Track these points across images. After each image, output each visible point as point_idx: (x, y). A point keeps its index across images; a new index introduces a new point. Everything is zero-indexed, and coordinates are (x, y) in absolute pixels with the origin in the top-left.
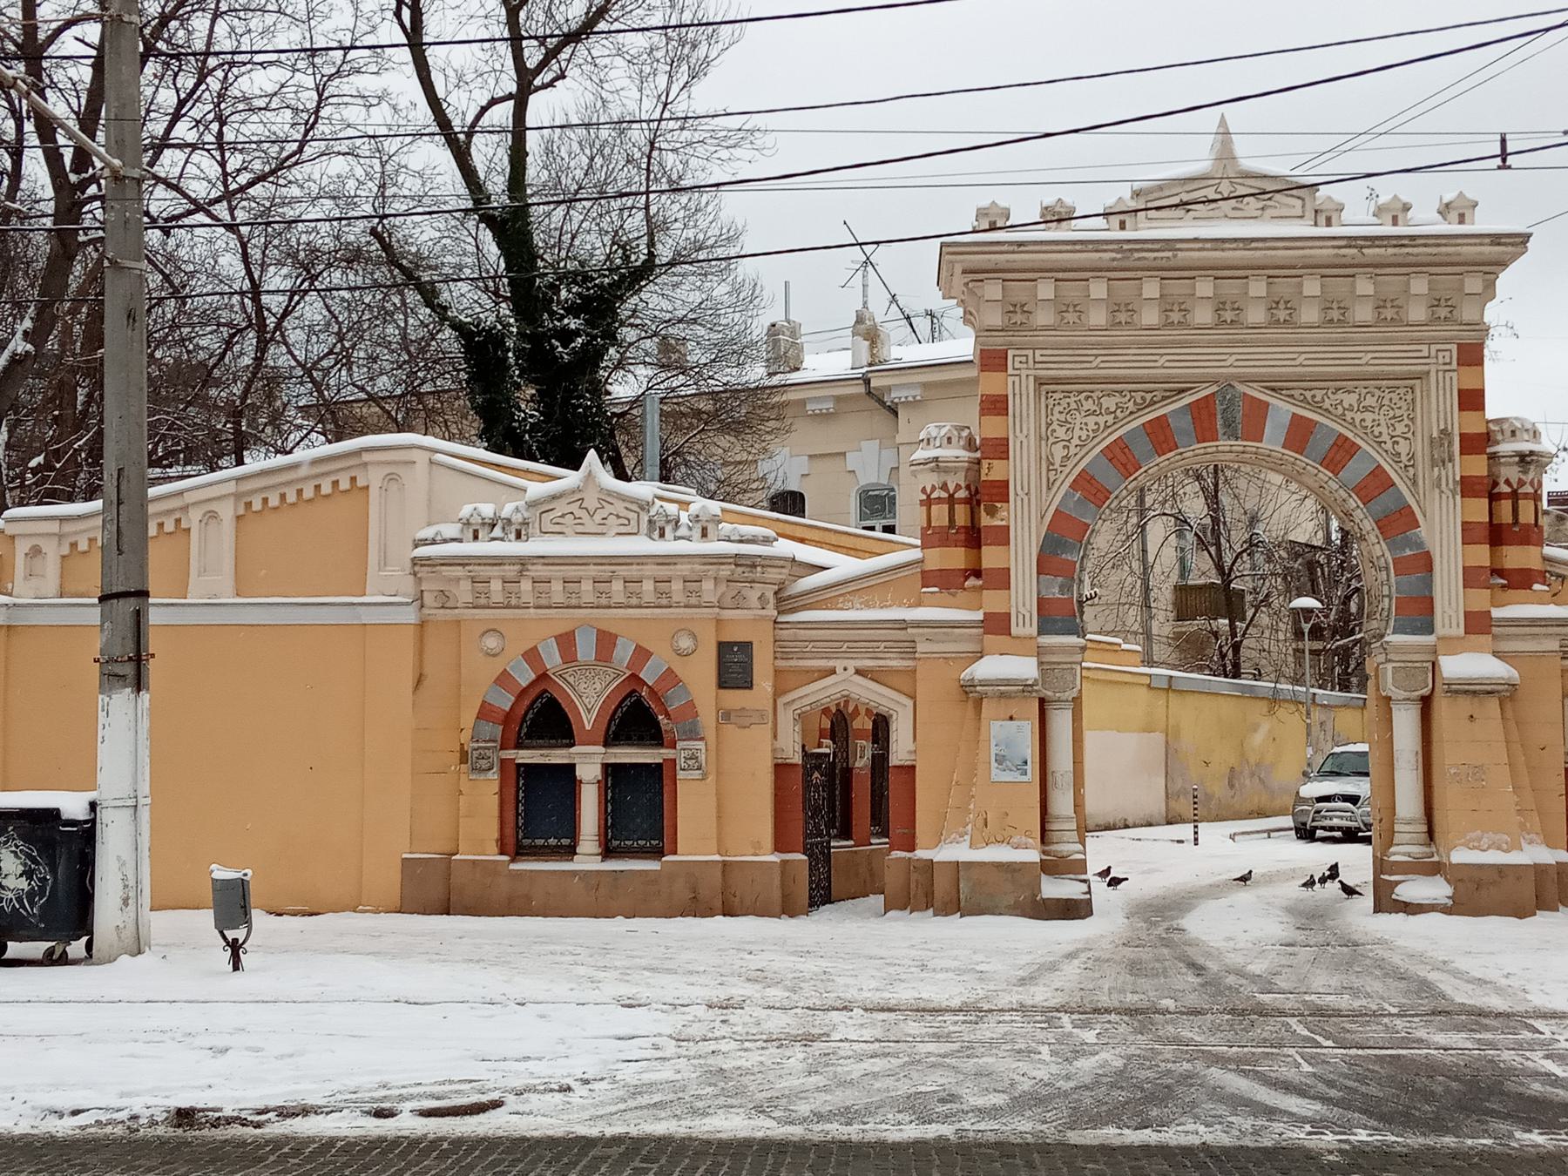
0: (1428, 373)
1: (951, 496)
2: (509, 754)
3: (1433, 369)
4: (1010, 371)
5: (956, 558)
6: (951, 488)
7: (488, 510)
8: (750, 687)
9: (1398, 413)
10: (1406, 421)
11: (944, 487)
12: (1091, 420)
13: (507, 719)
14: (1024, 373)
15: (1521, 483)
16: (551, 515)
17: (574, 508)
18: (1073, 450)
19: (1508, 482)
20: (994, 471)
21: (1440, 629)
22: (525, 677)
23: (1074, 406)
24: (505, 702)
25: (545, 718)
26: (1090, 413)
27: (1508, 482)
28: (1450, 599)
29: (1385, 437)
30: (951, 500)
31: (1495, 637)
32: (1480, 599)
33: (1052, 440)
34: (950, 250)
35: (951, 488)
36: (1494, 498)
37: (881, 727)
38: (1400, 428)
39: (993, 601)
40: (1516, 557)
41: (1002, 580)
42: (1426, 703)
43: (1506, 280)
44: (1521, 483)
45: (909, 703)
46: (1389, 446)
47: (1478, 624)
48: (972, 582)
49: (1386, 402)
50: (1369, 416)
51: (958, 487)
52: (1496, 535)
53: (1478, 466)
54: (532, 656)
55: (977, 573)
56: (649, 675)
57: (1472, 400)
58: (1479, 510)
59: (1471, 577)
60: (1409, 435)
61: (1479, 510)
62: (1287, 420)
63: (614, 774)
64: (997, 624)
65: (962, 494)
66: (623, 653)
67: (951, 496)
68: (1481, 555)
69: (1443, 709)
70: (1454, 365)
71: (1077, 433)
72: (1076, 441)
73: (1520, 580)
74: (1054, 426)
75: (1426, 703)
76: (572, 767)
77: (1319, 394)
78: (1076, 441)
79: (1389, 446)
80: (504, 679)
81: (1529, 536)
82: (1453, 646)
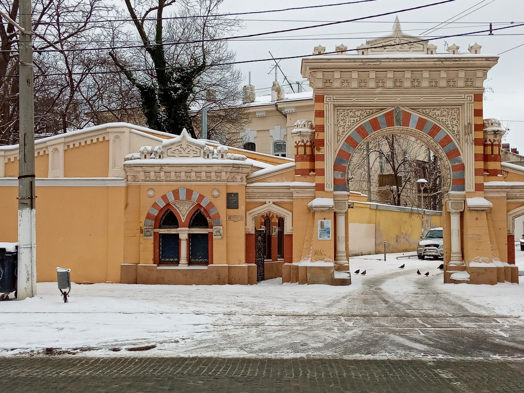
0: (464, 103)
1: (305, 144)
2: (157, 230)
3: (466, 102)
4: (325, 102)
5: (306, 165)
6: (305, 142)
7: (149, 148)
8: (238, 208)
10: (457, 120)
11: (303, 141)
12: (352, 119)
13: (156, 219)
14: (329, 103)
15: (494, 141)
16: (171, 150)
17: (179, 148)
18: (346, 129)
19: (490, 140)
20: (319, 136)
21: (467, 189)
22: (162, 204)
23: (346, 114)
24: (155, 213)
25: (169, 218)
26: (352, 117)
27: (490, 140)
28: (470, 179)
29: (450, 125)
30: (305, 146)
31: (485, 192)
32: (480, 179)
33: (339, 126)
34: (305, 61)
35: (305, 142)
36: (485, 146)
37: (281, 222)
38: (455, 122)
39: (319, 180)
40: (492, 165)
41: (322, 172)
42: (462, 214)
43: (490, 73)
44: (494, 141)
45: (291, 214)
46: (451, 128)
47: (479, 187)
48: (312, 173)
50: (444, 118)
51: (307, 141)
52: (486, 158)
53: (480, 135)
54: (164, 197)
55: (314, 170)
56: (204, 204)
57: (479, 113)
58: (480, 150)
59: (477, 172)
60: (458, 125)
61: (480, 150)
63: (191, 237)
64: (320, 187)
65: (308, 144)
66: (195, 197)
67: (305, 144)
68: (481, 165)
69: (467, 216)
70: (473, 101)
71: (347, 123)
72: (347, 126)
73: (494, 173)
74: (340, 121)
75: (462, 214)
76: (178, 235)
77: (428, 111)
78: (347, 126)
79: (451, 128)
80: (155, 205)
81: (497, 158)
82: (471, 195)
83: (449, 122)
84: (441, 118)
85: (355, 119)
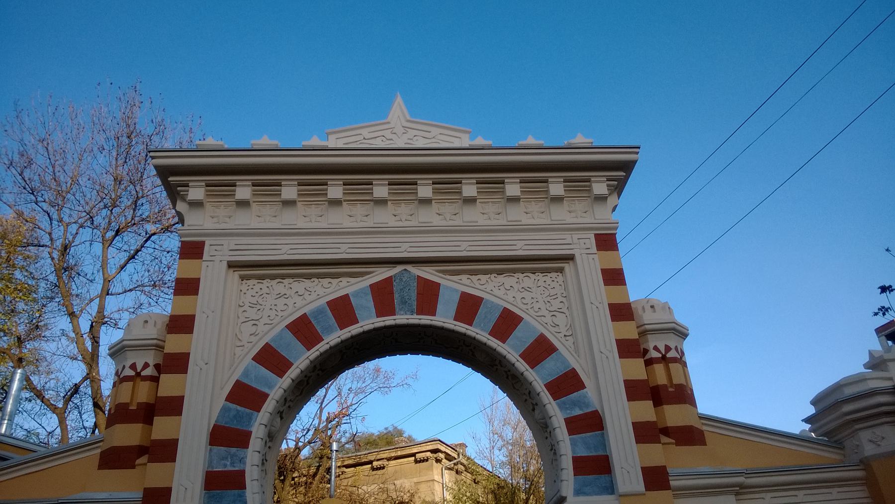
4: (205, 257)
9: (553, 292)
12: (282, 301)
23: (265, 290)
26: (280, 296)
36: (649, 363)
38: (556, 305)
40: (674, 415)
41: (166, 451)
44: (668, 349)
46: (548, 319)
48: (143, 459)
49: (541, 283)
51: (146, 365)
53: (629, 331)
57: (614, 277)
58: (636, 369)
59: (645, 433)
60: (564, 310)
61: (636, 369)
62: (457, 298)
65: (148, 372)
68: (646, 410)
70: (594, 250)
74: (246, 308)
77: (484, 278)
78: (263, 321)
79: (548, 319)
83: (541, 305)
84: (519, 296)
85: (290, 302)
